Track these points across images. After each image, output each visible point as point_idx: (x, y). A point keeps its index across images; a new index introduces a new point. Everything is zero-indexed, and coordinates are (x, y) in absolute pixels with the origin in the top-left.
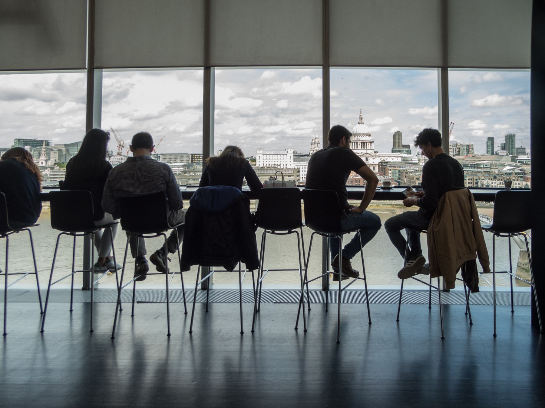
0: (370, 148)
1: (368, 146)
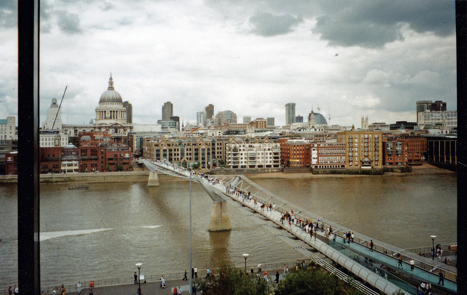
0: (122, 117)
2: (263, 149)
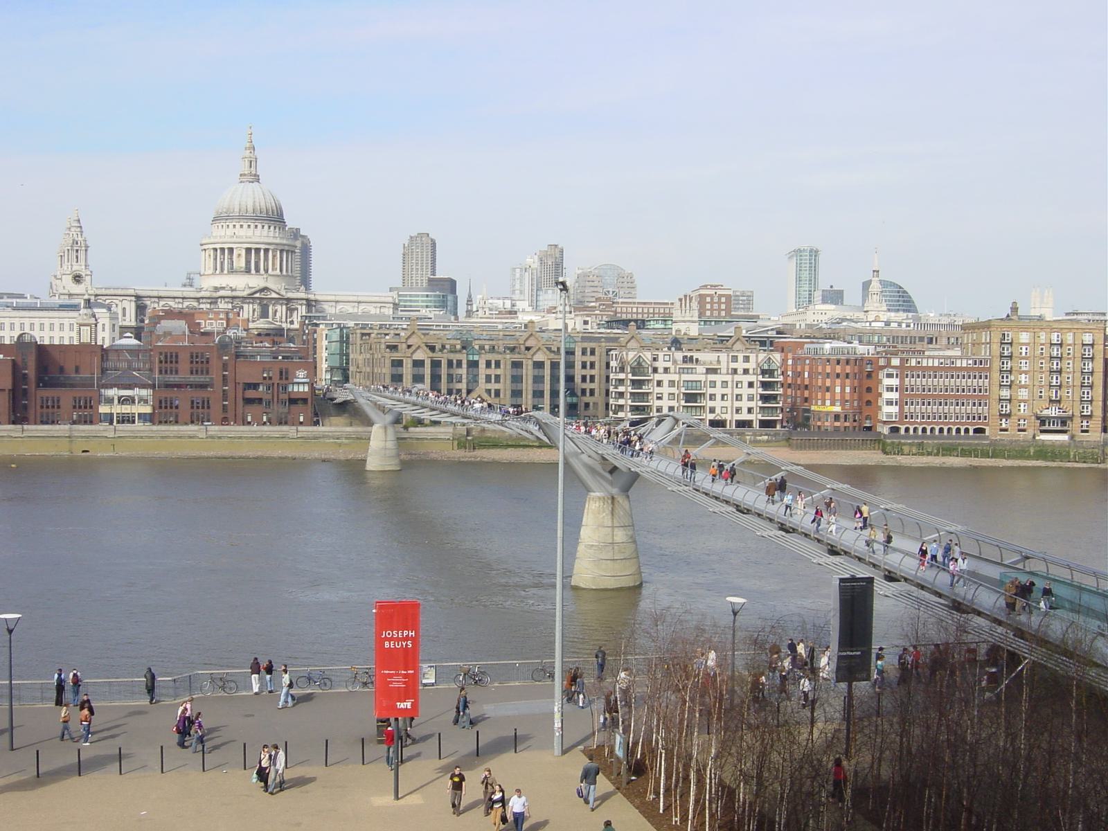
0: (281, 270)
2: (728, 369)
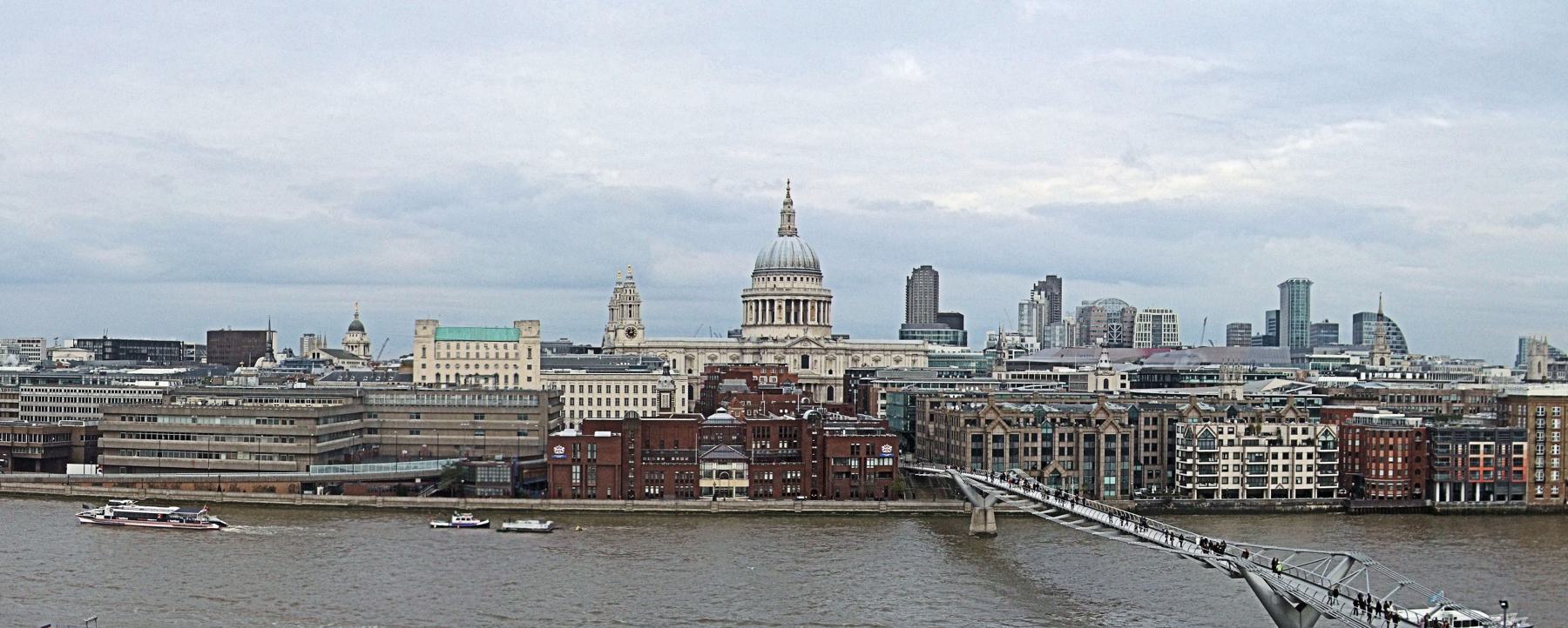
0: (818, 321)
1: (812, 315)
2: (1288, 441)
